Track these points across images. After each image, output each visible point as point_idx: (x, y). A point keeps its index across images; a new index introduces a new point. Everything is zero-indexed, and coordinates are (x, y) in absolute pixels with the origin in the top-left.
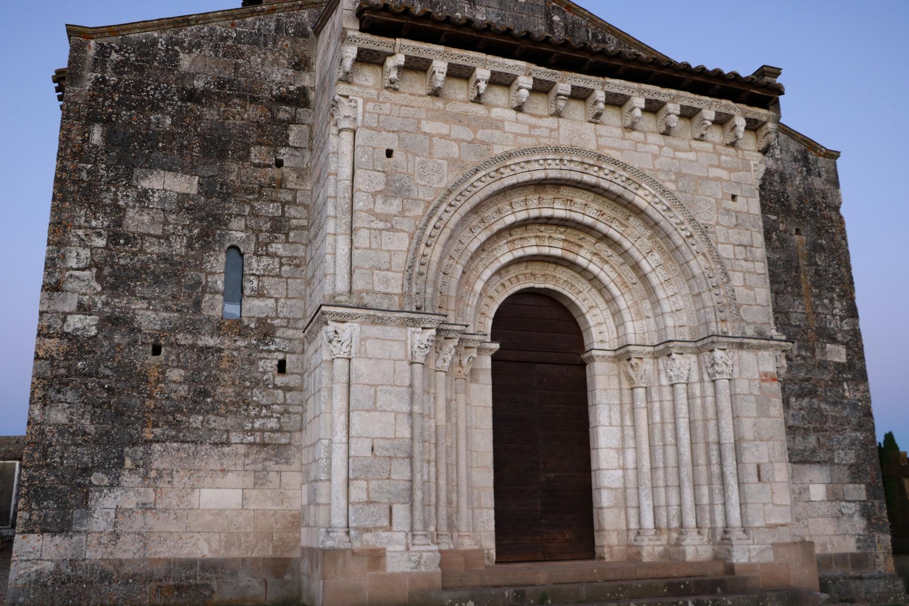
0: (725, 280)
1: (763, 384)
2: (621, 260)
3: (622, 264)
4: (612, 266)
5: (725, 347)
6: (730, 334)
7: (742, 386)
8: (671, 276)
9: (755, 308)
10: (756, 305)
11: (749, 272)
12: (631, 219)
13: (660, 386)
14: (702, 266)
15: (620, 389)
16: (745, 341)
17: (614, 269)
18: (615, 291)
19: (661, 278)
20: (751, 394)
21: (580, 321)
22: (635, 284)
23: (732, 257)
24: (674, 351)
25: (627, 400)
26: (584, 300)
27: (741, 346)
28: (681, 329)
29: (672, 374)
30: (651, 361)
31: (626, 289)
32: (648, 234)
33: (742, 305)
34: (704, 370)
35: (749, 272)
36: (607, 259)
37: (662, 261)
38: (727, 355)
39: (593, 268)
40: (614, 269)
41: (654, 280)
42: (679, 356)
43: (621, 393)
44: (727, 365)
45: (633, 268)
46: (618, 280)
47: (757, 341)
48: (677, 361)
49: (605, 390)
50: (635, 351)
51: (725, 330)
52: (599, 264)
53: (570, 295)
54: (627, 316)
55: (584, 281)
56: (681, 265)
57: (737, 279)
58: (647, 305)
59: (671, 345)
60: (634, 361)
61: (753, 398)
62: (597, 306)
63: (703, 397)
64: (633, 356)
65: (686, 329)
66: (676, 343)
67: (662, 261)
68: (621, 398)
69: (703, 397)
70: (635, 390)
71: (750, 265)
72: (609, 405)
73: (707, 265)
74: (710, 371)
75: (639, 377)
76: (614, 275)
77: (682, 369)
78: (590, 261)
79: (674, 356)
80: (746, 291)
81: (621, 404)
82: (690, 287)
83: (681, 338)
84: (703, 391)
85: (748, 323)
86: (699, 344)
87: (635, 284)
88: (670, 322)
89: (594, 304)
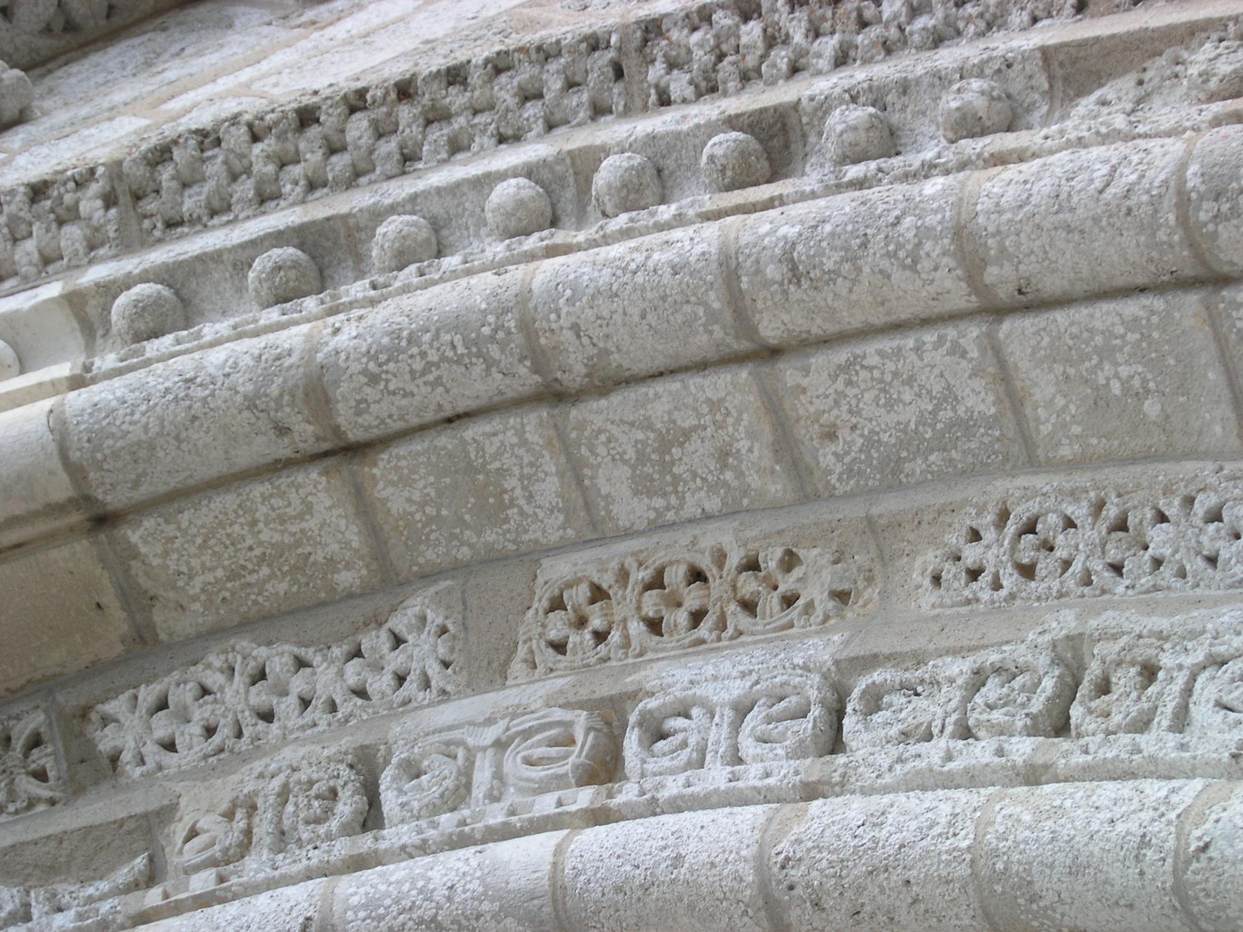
12: (126, 728)
32: (423, 651)
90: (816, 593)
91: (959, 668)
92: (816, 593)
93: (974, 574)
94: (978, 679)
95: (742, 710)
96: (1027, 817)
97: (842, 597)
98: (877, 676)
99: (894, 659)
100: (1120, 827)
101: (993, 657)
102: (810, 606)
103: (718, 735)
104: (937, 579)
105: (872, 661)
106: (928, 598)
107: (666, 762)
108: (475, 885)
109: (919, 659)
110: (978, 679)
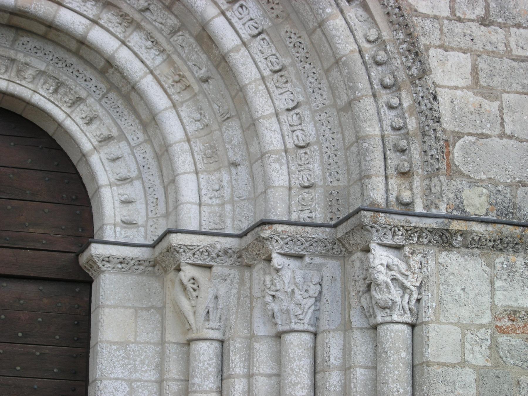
0: (414, 71)
1: (502, 339)
2: (172, 21)
3: (174, 32)
4: (149, 36)
5: (399, 240)
6: (419, 209)
7: (442, 341)
8: (287, 61)
9: (495, 143)
10: (502, 135)
11: (491, 54)
13: (252, 337)
14: (360, 35)
15: (162, 343)
16: (456, 226)
17: (155, 42)
18: (158, 98)
19: (262, 65)
20: (463, 364)
21: (82, 170)
22: (206, 80)
23: (446, 13)
24: (275, 248)
25: (174, 370)
26: (90, 122)
27: (444, 239)
28: (306, 195)
29: (275, 307)
30: (235, 273)
31: (186, 95)
33: (459, 136)
34: (354, 302)
35: (491, 54)
36: (137, 17)
37: (266, 24)
38: (406, 260)
39: (98, 37)
40: (155, 42)
41: (247, 69)
42: (294, 263)
43: (162, 355)
44: (404, 288)
45: (199, 39)
46: (166, 70)
47: (490, 228)
48: (287, 275)
49: (123, 344)
50: (188, 248)
51: (406, 196)
52: (118, 30)
53: (49, 107)
54: (183, 161)
55: (89, 73)
56: (311, 33)
57: (449, 71)
58: (233, 132)
59: (266, 232)
60: (188, 272)
61: (469, 376)
62: (122, 137)
63: (346, 369)
64: (183, 258)
65: (317, 194)
66: (280, 228)
67: (266, 24)
68: (160, 368)
69: (346, 369)
70: (193, 346)
71: (497, 35)
72: (130, 382)
73: (373, 34)
74: (364, 302)
75: (202, 312)
76: (153, 58)
77: (298, 296)
78: (95, 22)
79: (277, 260)
80: (473, 99)
81: (160, 382)
82: (332, 88)
83: (304, 216)
84: (347, 351)
85: (473, 183)
86: (341, 231)
87: (206, 81)
88: (279, 175)
89: (115, 132)
90: (276, 12)
91: (274, 52)
92: (276, 12)
93: (290, 38)
94: (274, 55)
95: (251, 19)
96: (253, 90)
97: (277, 16)
98: (267, 38)
99: (270, 39)
100: (258, 107)
101: (278, 55)
102: (273, 13)
103: (246, 19)
104: (287, 32)
105: (268, 35)
106: (283, 33)
107: (237, 14)
108: (200, 10)
109: (272, 42)
110: (274, 55)
